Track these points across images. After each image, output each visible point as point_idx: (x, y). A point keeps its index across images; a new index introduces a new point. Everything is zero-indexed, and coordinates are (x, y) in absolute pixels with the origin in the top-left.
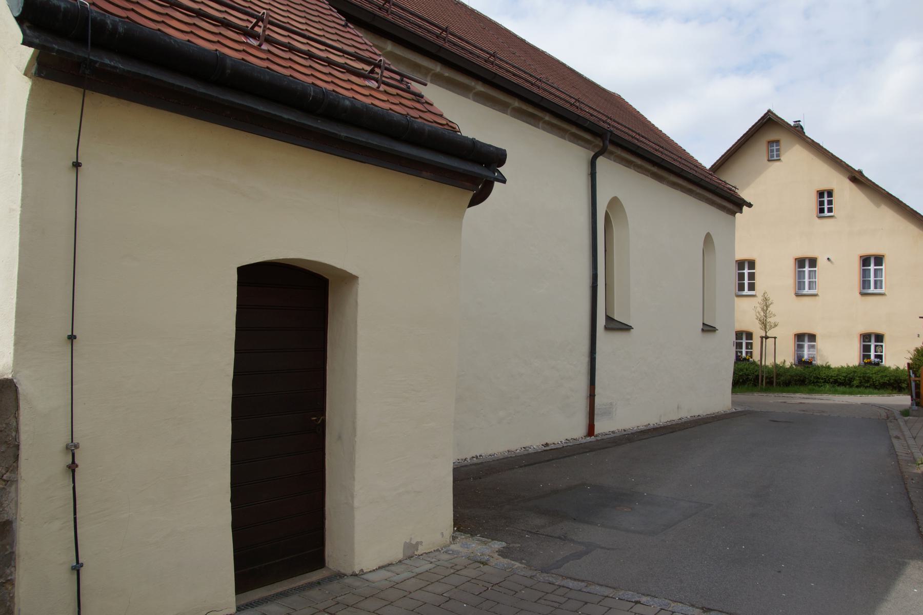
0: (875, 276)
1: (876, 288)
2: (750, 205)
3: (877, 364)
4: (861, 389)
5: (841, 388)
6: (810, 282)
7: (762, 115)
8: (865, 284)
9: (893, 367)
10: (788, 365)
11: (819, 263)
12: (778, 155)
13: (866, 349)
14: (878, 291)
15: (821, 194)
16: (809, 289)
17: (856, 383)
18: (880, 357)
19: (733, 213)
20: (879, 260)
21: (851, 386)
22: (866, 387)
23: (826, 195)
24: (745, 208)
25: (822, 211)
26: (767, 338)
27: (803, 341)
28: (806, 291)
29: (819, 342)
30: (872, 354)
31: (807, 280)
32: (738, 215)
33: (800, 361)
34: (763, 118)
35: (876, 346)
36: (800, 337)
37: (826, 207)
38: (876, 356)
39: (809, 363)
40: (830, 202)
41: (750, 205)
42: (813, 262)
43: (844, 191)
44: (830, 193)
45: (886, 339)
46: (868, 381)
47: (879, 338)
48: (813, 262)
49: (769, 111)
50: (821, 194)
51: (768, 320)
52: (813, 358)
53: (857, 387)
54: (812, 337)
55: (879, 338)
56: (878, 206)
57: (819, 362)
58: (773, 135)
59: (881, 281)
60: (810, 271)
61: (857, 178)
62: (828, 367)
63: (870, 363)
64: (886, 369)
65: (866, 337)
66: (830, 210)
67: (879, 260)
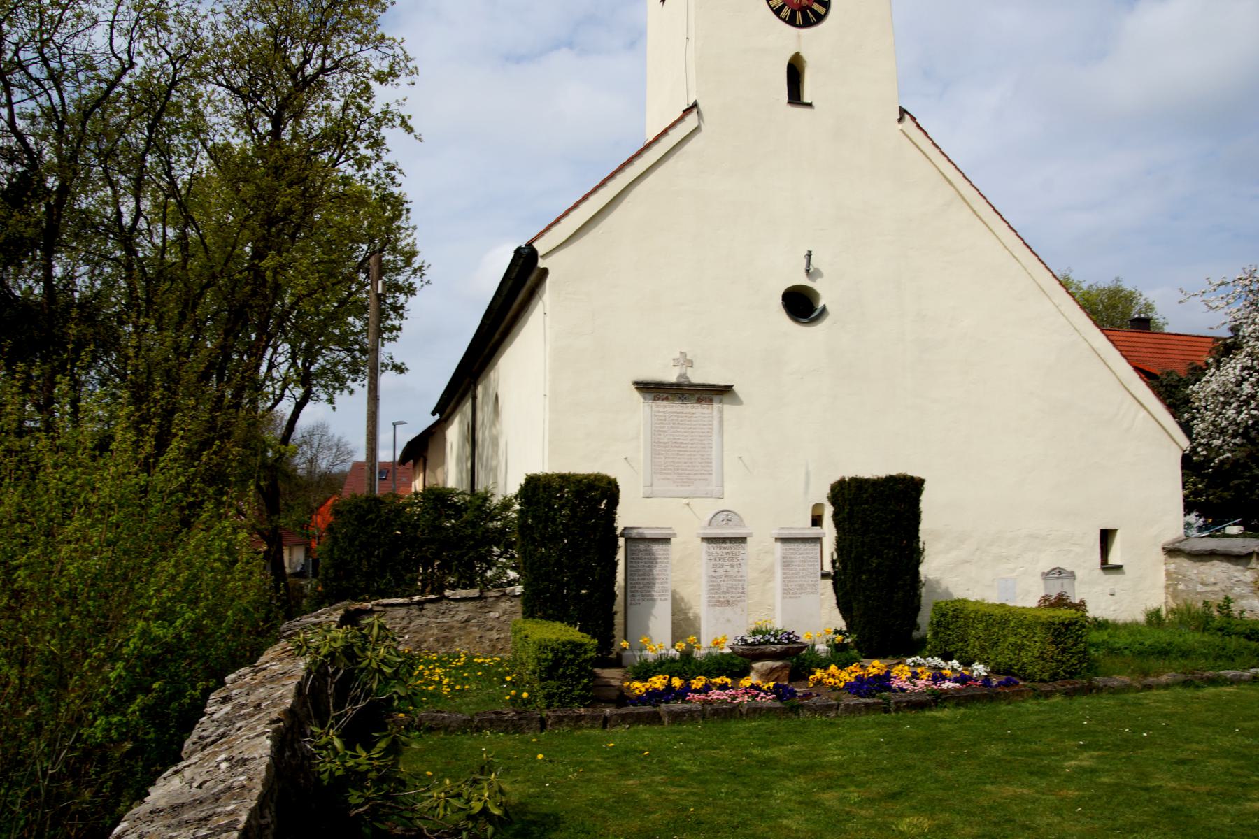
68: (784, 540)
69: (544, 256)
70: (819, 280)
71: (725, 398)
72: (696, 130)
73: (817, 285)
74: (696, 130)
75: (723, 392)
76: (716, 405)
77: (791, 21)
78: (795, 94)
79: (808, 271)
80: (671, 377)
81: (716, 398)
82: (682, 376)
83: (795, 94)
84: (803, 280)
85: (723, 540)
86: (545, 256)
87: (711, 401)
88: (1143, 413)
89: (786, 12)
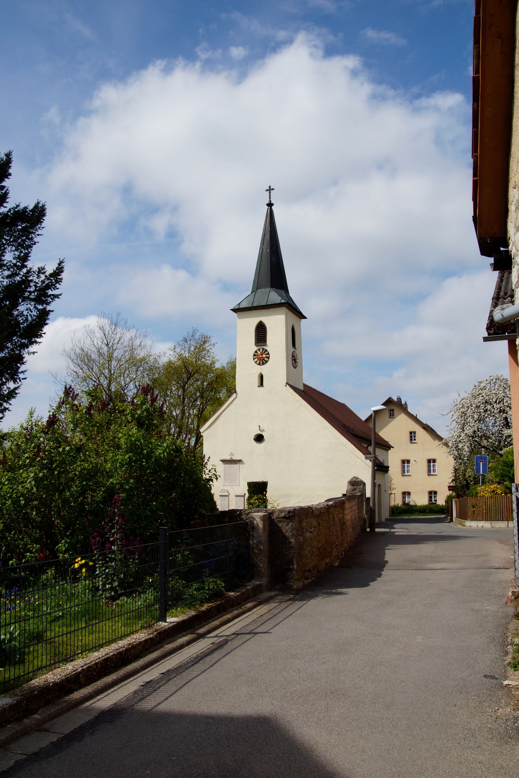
0: (433, 467)
1: (433, 472)
2: (393, 448)
3: (435, 503)
4: (429, 514)
5: (422, 514)
6: (407, 470)
7: (387, 399)
8: (429, 471)
9: (441, 504)
10: (400, 505)
11: (411, 462)
12: (393, 416)
13: (430, 497)
14: (434, 473)
15: (411, 433)
16: (407, 473)
17: (427, 511)
18: (436, 501)
19: (388, 450)
20: (434, 461)
21: (425, 513)
22: (431, 513)
23: (413, 433)
24: (391, 448)
25: (411, 440)
26: (391, 494)
27: (405, 495)
28: (406, 474)
29: (412, 495)
30: (433, 499)
31: (406, 469)
32: (389, 451)
33: (404, 503)
34: (387, 400)
35: (434, 496)
36: (404, 493)
37: (413, 438)
38: (435, 500)
39: (408, 504)
40: (415, 436)
41: (393, 448)
42: (408, 461)
43: (421, 433)
44: (415, 433)
45: (438, 493)
46: (432, 511)
47: (435, 493)
48: (408, 461)
49: (390, 397)
50: (411, 433)
51: (392, 486)
52: (410, 502)
53: (428, 513)
54: (409, 493)
55: (435, 493)
56: (435, 440)
57: (412, 503)
58: (392, 407)
59: (435, 470)
60: (407, 465)
61: (427, 428)
62: (416, 506)
63: (432, 503)
64: (438, 505)
65: (430, 493)
66: (415, 440)
67: (434, 461)
68: (236, 496)
69: (203, 432)
70: (263, 432)
71: (240, 462)
72: (236, 397)
73: (263, 434)
74: (236, 397)
75: (239, 461)
76: (238, 465)
77: (259, 364)
78: (261, 384)
79: (260, 430)
80: (228, 458)
81: (238, 463)
82: (231, 458)
83: (261, 384)
84: (260, 432)
85: (223, 496)
86: (203, 432)
87: (237, 464)
88: (359, 460)
89: (258, 362)
